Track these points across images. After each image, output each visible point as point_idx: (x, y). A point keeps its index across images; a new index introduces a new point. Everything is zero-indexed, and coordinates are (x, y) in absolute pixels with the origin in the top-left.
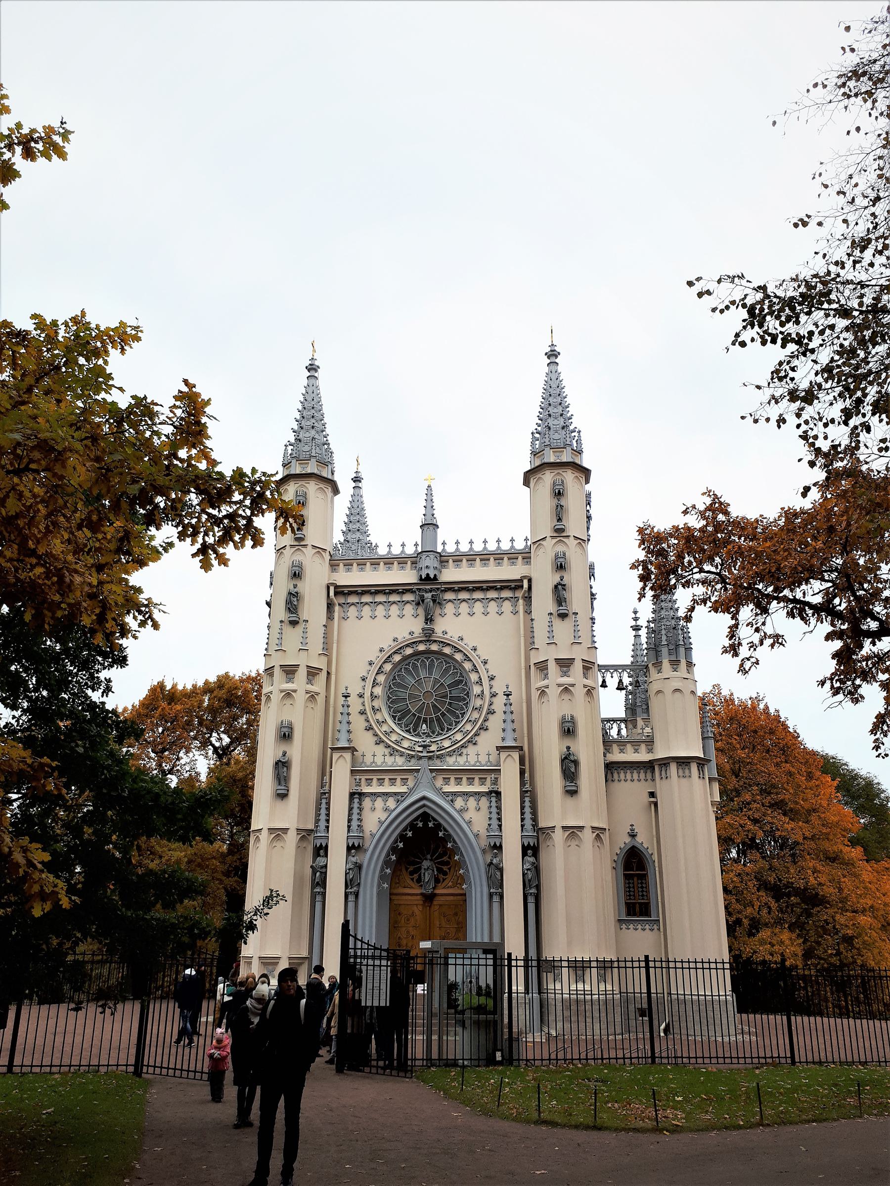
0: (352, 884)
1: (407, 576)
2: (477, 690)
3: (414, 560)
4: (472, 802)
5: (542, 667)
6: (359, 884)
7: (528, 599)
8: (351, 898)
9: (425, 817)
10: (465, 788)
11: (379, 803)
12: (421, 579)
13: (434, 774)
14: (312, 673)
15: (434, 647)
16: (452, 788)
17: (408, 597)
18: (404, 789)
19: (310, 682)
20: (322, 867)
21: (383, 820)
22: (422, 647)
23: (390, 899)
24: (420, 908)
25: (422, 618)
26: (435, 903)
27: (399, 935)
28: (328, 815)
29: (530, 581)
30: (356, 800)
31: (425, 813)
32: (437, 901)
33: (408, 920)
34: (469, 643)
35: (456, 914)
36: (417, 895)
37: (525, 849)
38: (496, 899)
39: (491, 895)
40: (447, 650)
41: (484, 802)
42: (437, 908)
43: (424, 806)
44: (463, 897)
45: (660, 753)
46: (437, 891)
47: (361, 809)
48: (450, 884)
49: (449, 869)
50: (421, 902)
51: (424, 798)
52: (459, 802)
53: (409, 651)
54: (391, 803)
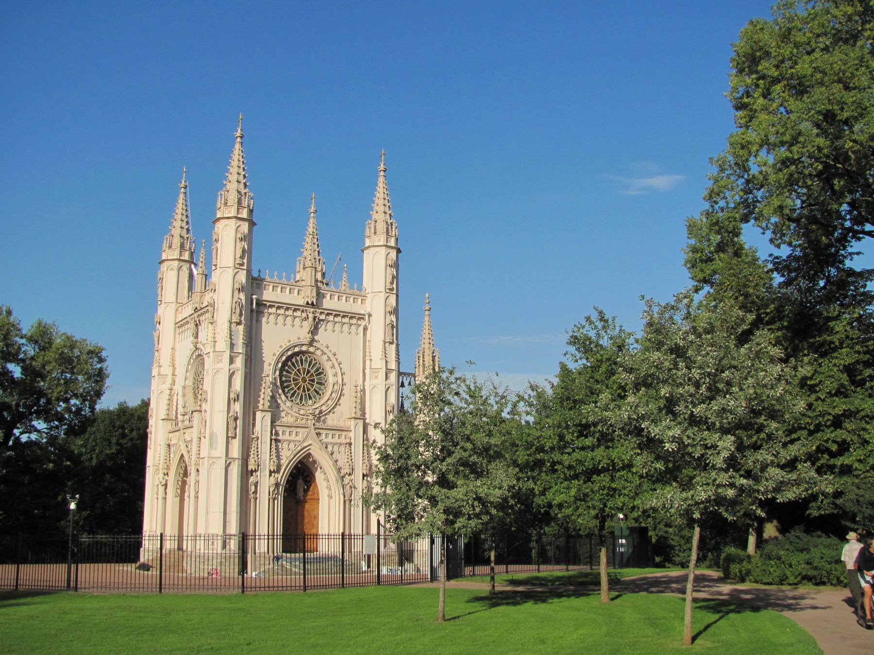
2: (331, 380)
12: (308, 303)
15: (312, 349)
17: (298, 313)
18: (297, 438)
22: (304, 348)
29: (370, 315)
30: (273, 443)
37: (364, 476)
38: (347, 502)
39: (345, 501)
41: (342, 448)
52: (330, 448)
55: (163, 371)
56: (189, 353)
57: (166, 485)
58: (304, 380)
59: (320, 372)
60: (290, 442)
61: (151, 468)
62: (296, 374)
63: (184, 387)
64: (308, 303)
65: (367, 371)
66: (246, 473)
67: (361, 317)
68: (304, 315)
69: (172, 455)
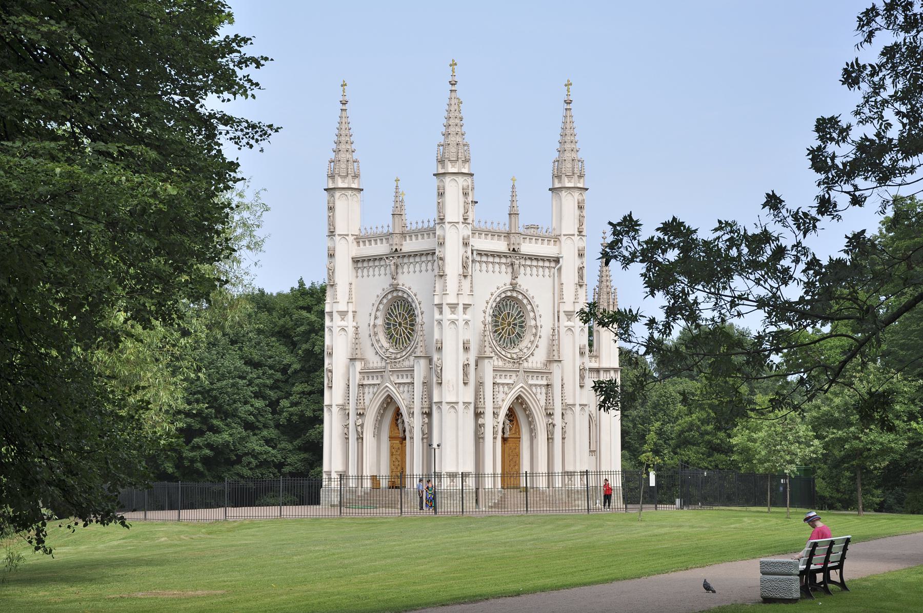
1: (500, 246)
3: (508, 235)
5: (569, 314)
7: (560, 269)
10: (534, 382)
12: (514, 250)
14: (466, 307)
15: (515, 294)
16: (530, 382)
17: (503, 260)
18: (511, 381)
19: (464, 313)
22: (509, 294)
25: (509, 276)
34: (531, 293)
40: (520, 297)
45: (605, 365)
53: (503, 295)
54: (506, 388)
55: (342, 307)
56: (379, 291)
57: (362, 426)
58: (509, 325)
59: (521, 315)
60: (503, 384)
61: (335, 409)
62: (503, 319)
63: (375, 326)
64: (514, 250)
65: (562, 315)
66: (478, 415)
67: (557, 260)
68: (509, 260)
69: (368, 397)
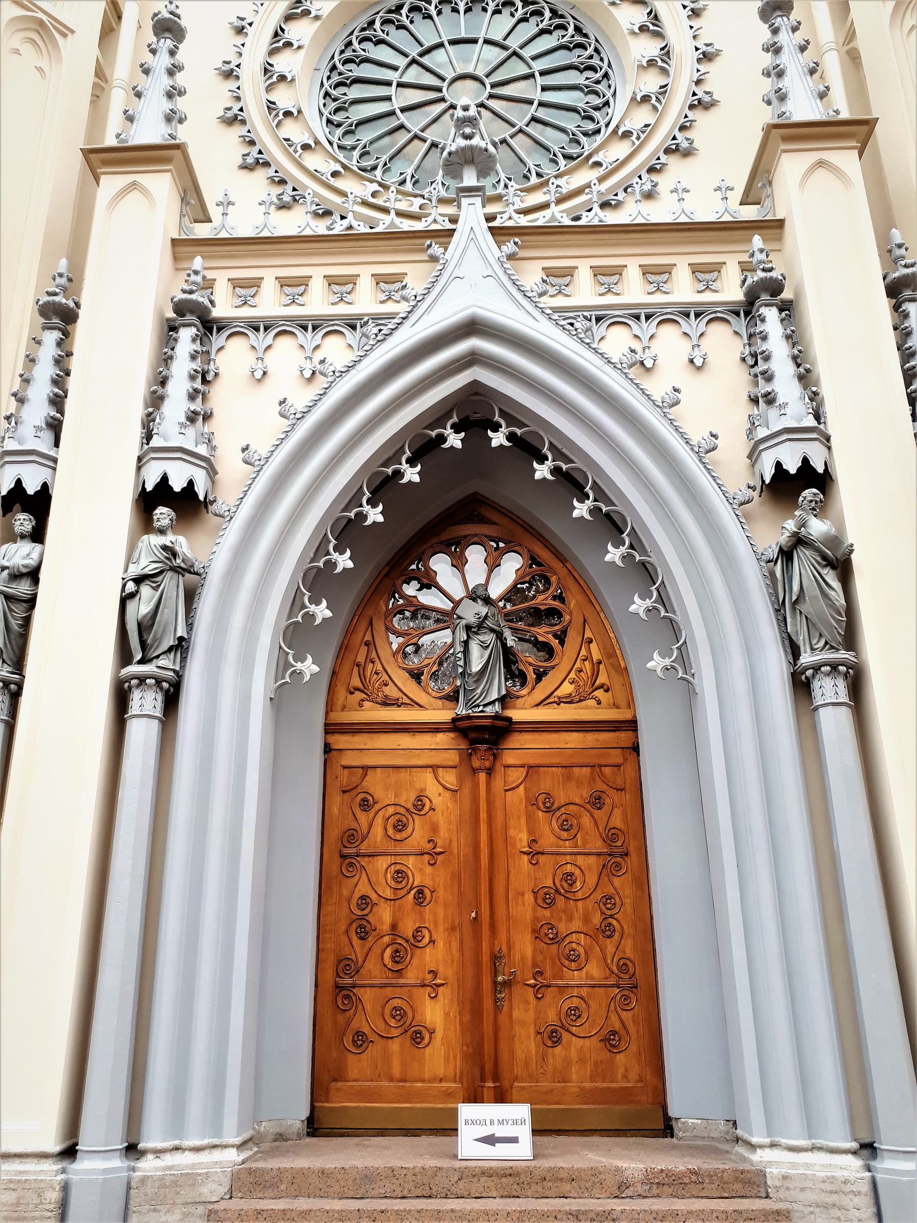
0: (150, 661)
4: (669, 345)
6: (181, 646)
8: (145, 702)
9: (474, 410)
11: (286, 355)
13: (509, 248)
20: (16, 576)
21: (300, 406)
23: (328, 749)
24: (450, 778)
26: (509, 758)
27: (363, 888)
28: (59, 382)
30: (186, 335)
31: (476, 392)
32: (519, 750)
33: (400, 826)
35: (597, 801)
36: (434, 728)
38: (830, 689)
42: (516, 776)
43: (472, 359)
44: (624, 737)
46: (516, 715)
47: (205, 377)
48: (567, 688)
49: (561, 637)
50: (452, 757)
51: (472, 327)
